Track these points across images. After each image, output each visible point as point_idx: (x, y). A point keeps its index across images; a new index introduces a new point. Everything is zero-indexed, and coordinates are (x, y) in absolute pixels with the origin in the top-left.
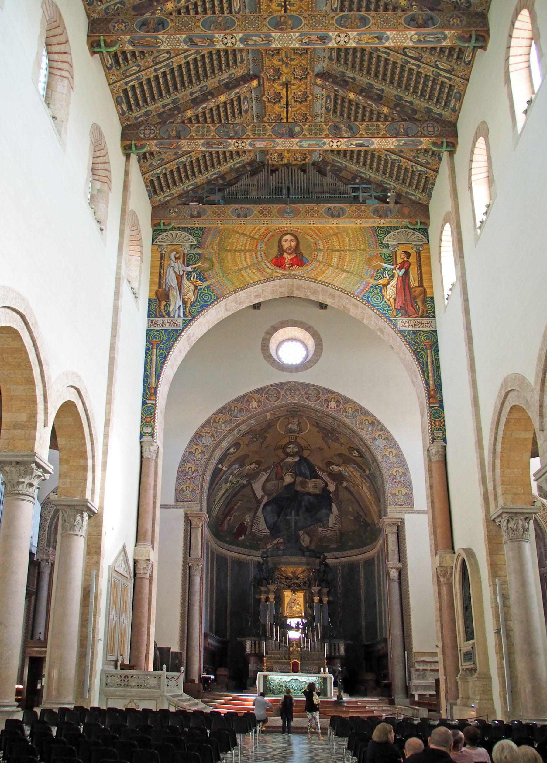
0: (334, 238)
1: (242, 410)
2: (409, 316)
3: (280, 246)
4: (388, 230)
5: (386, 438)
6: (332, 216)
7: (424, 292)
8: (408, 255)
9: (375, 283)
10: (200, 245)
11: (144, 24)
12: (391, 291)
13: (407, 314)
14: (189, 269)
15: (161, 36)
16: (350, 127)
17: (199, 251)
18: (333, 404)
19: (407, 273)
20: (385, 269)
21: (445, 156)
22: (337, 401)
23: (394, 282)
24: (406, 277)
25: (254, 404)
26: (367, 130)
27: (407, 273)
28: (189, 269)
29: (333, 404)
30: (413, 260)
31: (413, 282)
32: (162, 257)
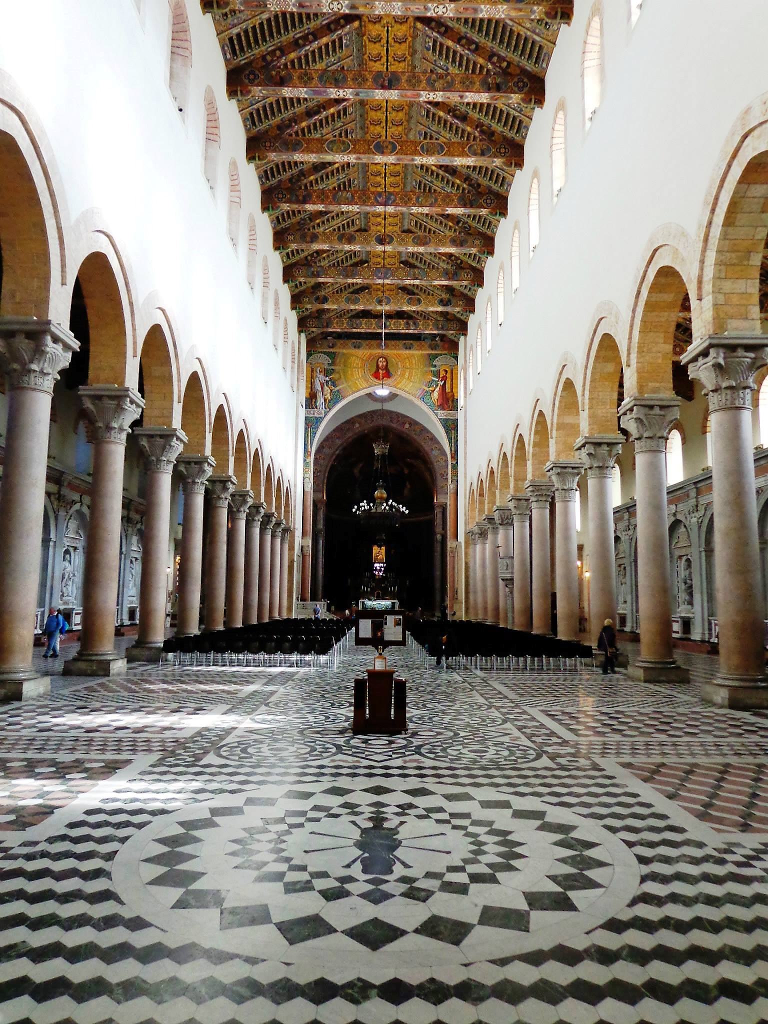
0: (407, 360)
1: (349, 429)
2: (444, 410)
3: (378, 365)
4: (436, 356)
5: (439, 450)
6: (406, 348)
7: (453, 396)
8: (446, 371)
9: (428, 389)
10: (333, 363)
11: (317, 299)
12: (436, 395)
13: (443, 409)
14: (327, 379)
15: (325, 305)
16: (415, 323)
17: (333, 368)
18: (407, 426)
19: (445, 384)
20: (433, 380)
21: (462, 338)
22: (410, 424)
23: (437, 389)
24: (444, 386)
25: (357, 425)
26: (423, 325)
27: (445, 384)
28: (327, 379)
29: (407, 426)
30: (448, 375)
31: (448, 390)
32: (312, 371)
